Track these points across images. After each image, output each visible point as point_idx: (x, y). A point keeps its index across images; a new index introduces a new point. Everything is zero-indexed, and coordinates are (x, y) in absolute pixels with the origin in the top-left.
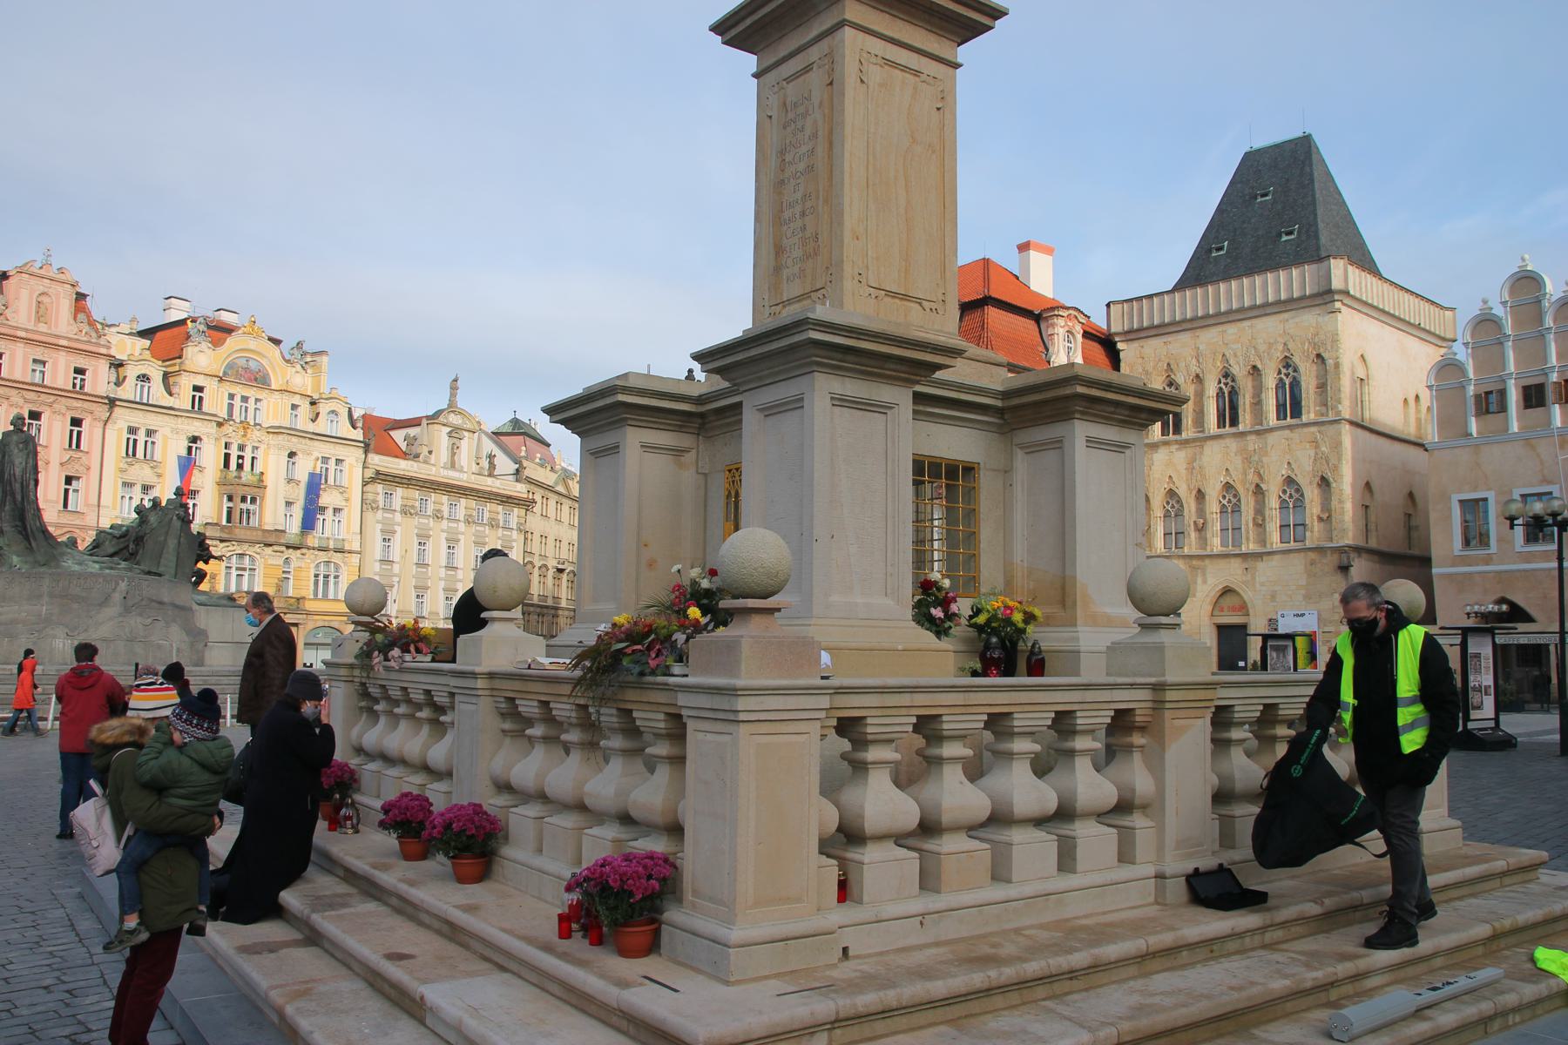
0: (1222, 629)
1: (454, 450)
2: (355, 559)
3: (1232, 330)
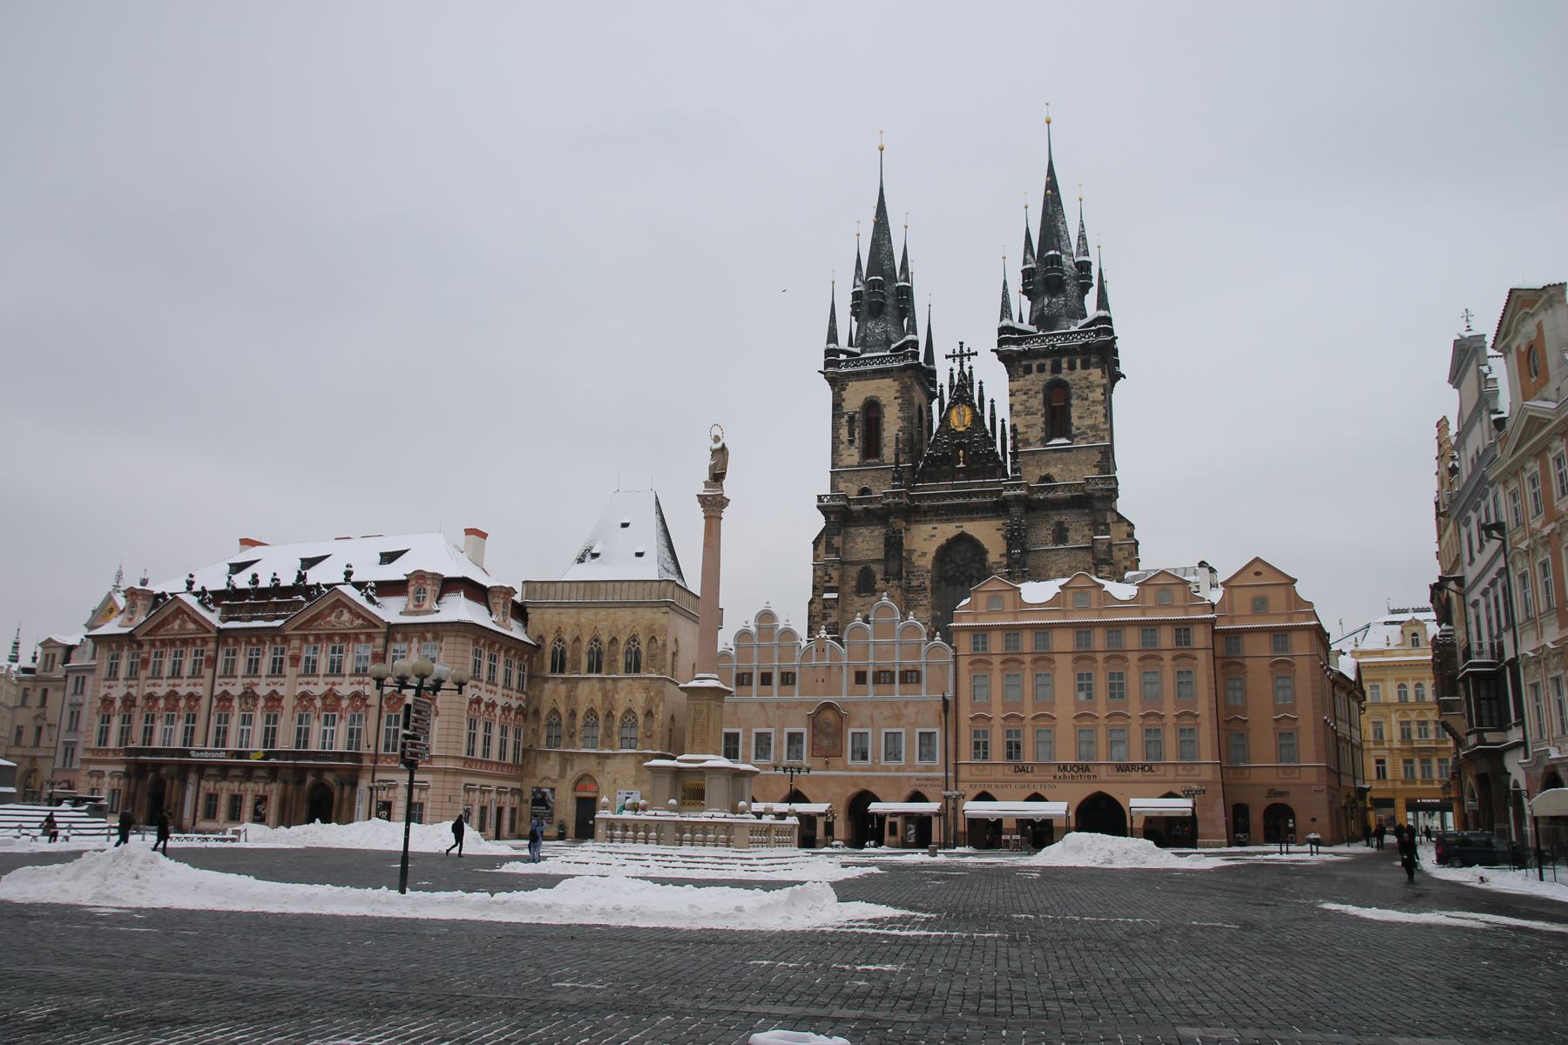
0: (580, 800)
3: (603, 613)
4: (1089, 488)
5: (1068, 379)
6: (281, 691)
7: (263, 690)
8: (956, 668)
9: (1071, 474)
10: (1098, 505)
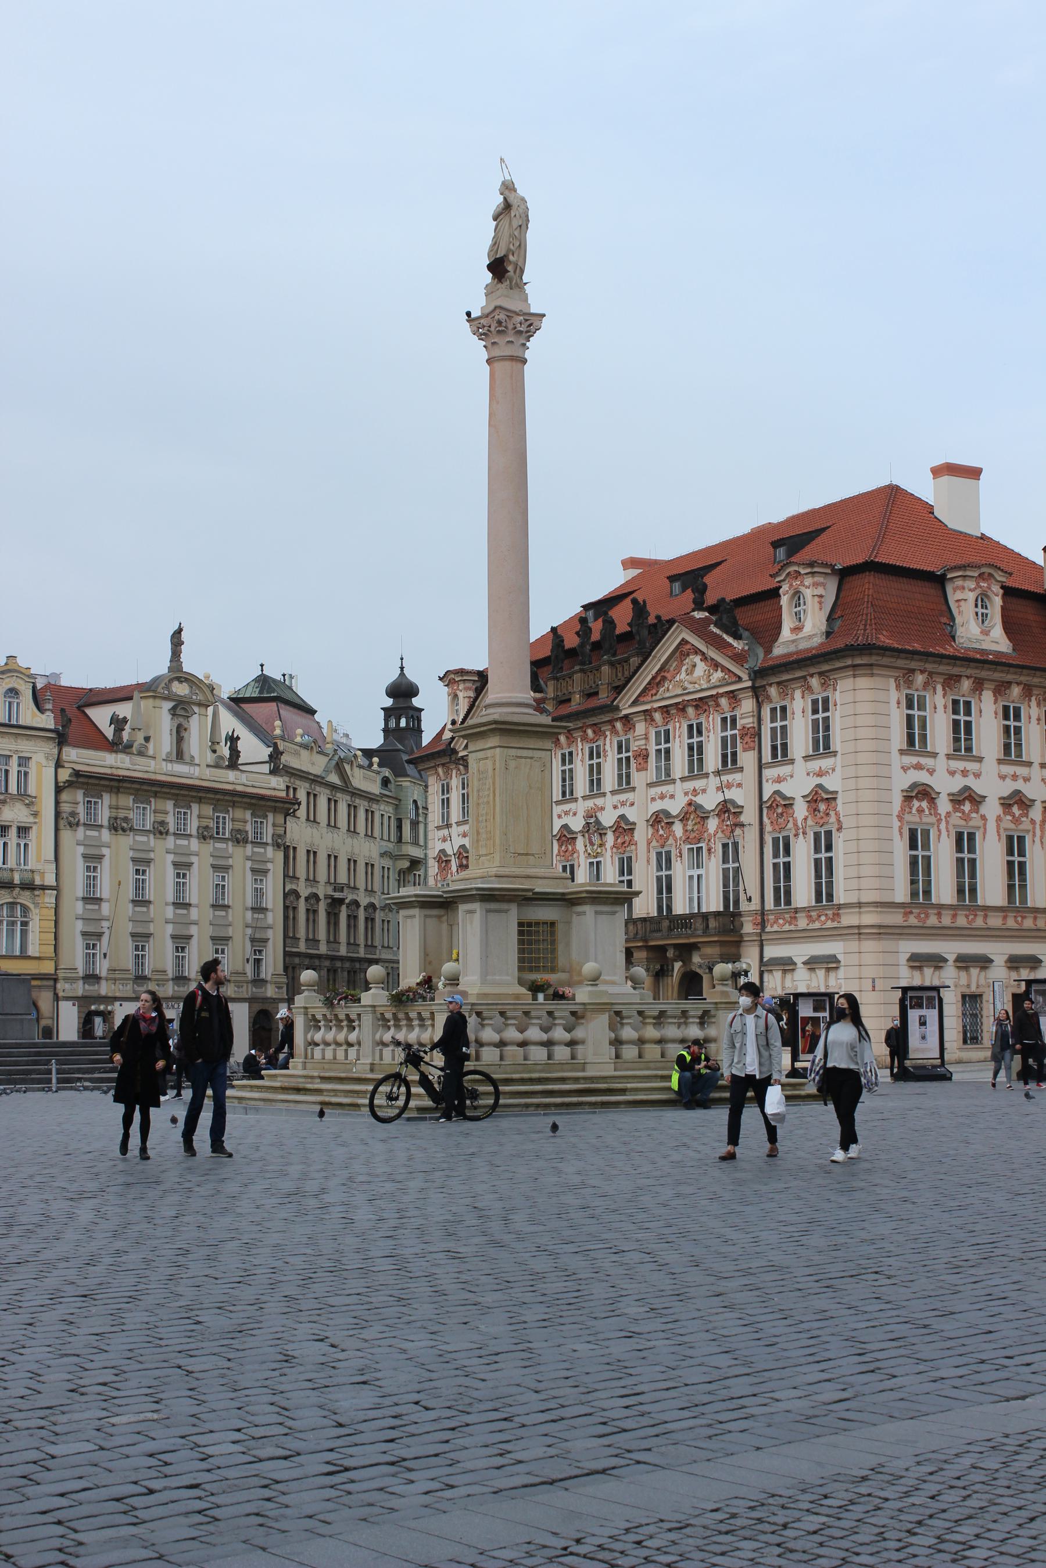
1: (180, 734)
2: (49, 898)
6: (632, 815)
7: (608, 819)
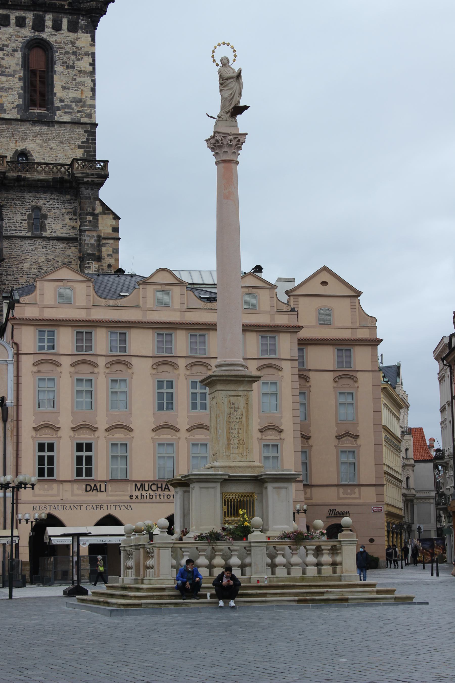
4: (78, 170)
5: (52, 39)
8: (18, 369)
9: (51, 149)
10: (86, 192)
